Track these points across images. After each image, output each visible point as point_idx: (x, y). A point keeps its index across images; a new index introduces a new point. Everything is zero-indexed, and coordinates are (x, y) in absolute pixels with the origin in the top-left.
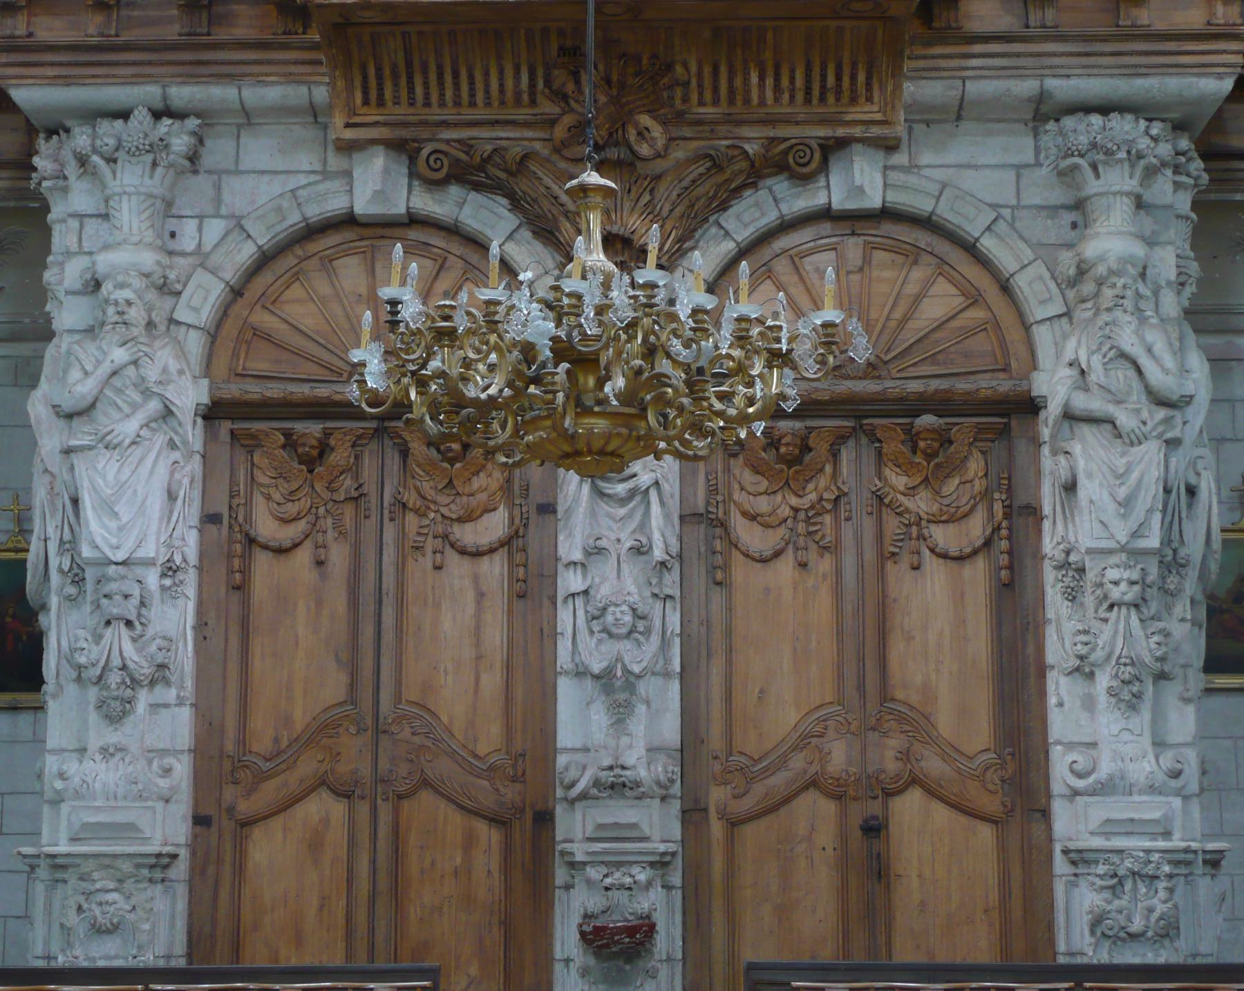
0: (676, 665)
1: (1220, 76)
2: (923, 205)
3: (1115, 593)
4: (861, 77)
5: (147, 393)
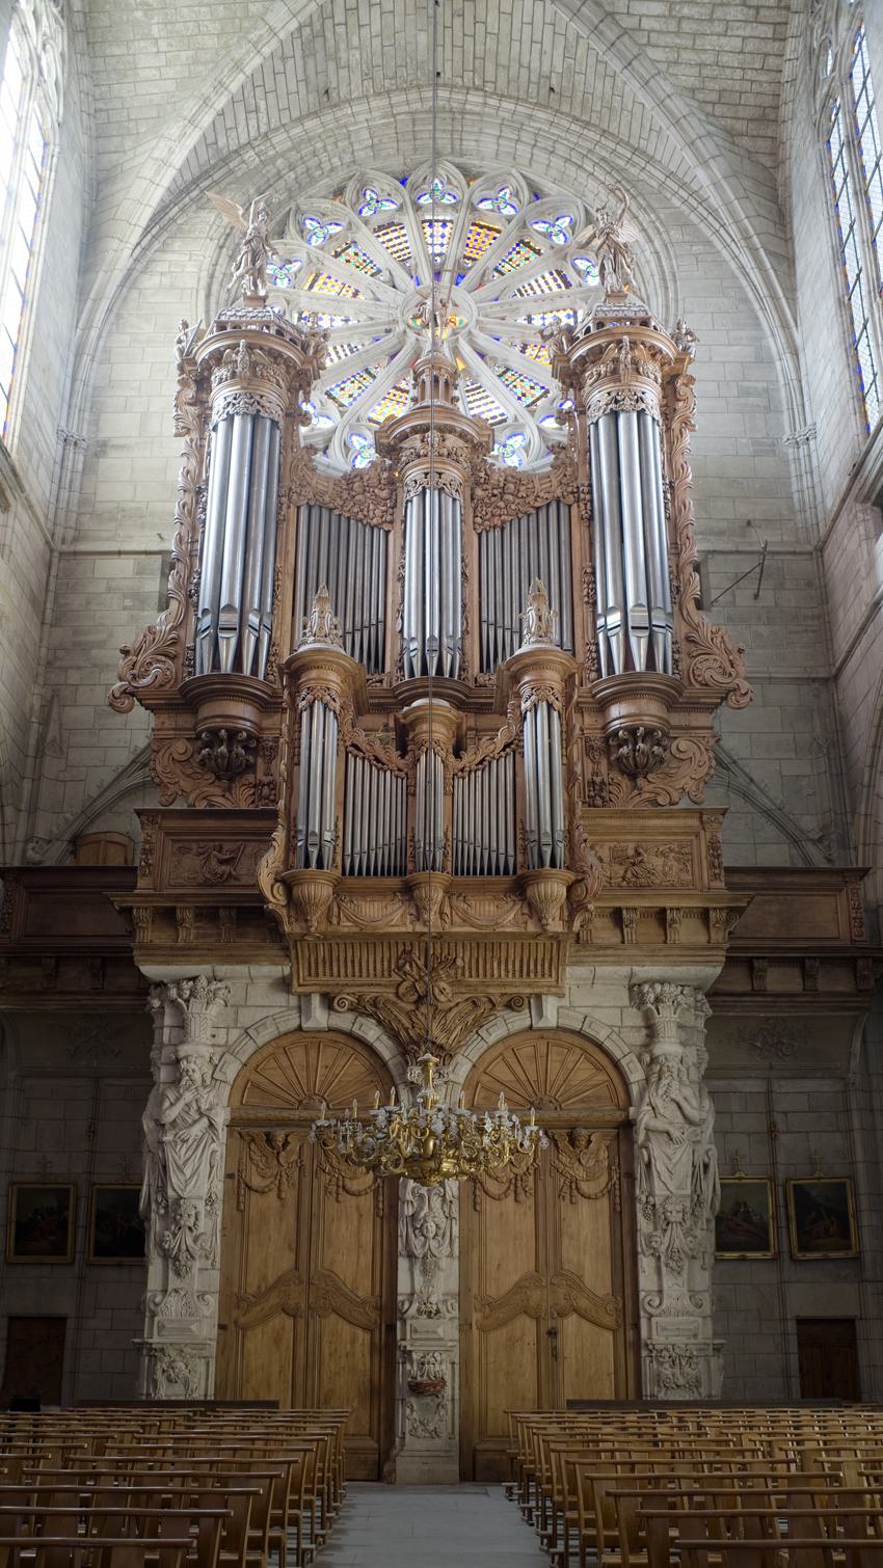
2: (578, 1026)
4: (547, 965)
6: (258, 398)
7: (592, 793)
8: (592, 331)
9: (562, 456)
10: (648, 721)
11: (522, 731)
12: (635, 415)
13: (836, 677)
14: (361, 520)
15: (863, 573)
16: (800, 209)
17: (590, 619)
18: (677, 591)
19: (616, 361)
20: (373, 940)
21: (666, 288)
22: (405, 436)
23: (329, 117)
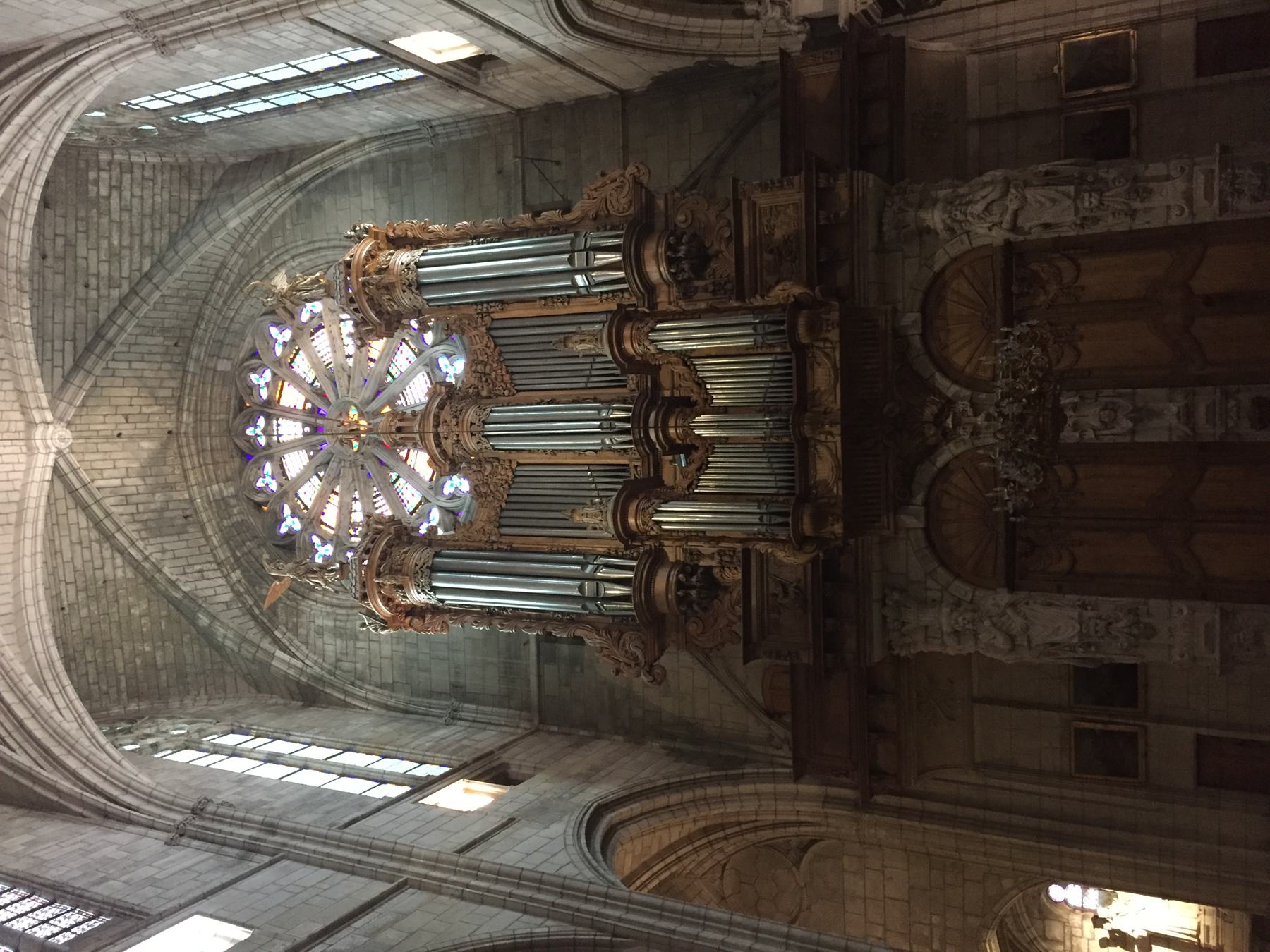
0: (1129, 390)
1: (868, 180)
3: (1095, 202)
5: (1004, 613)
6: (417, 568)
7: (722, 292)
8: (356, 306)
9: (454, 327)
10: (661, 250)
11: (673, 352)
12: (420, 270)
13: (622, 92)
14: (509, 485)
15: (535, 74)
16: (253, 143)
17: (581, 299)
18: (557, 229)
19: (378, 287)
20: (847, 469)
21: (320, 248)
22: (443, 453)
23: (204, 515)
